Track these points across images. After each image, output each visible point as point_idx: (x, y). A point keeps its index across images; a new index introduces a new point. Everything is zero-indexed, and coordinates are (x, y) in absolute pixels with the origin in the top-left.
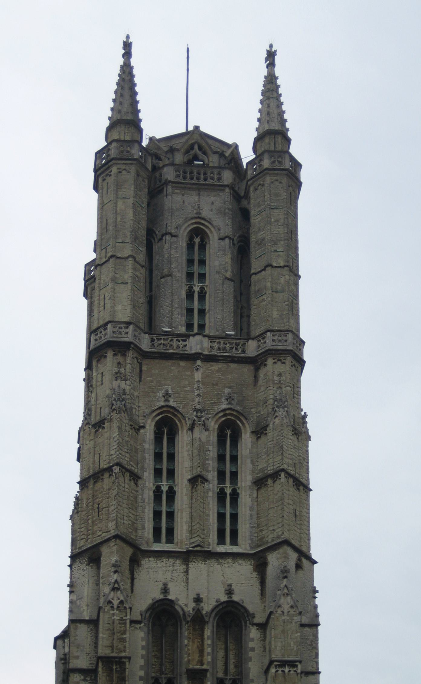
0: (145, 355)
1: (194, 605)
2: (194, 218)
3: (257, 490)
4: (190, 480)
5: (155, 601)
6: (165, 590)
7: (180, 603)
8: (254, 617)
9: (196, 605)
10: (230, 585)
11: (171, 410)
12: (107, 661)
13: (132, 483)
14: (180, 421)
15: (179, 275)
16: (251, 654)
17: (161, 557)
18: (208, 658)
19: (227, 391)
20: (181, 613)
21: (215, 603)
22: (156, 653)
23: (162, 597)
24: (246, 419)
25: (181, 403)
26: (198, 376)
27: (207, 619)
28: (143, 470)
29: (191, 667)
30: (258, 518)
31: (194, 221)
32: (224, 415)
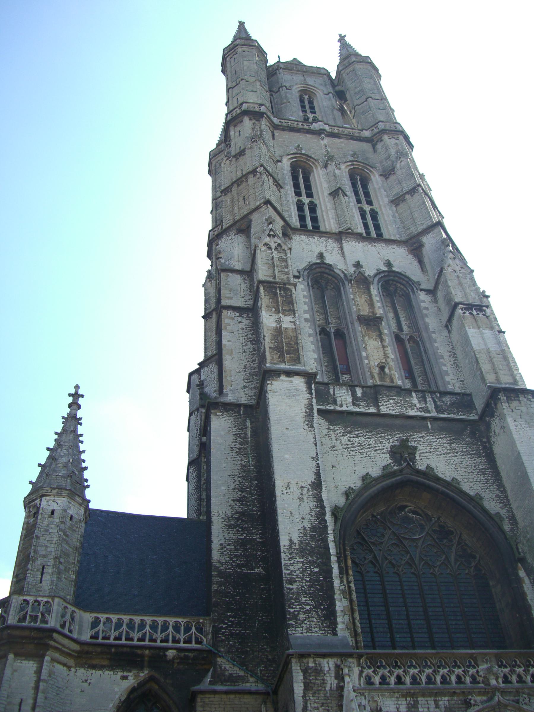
2: (302, 84)
3: (396, 206)
5: (311, 263)
8: (420, 285)
14: (313, 163)
16: (425, 312)
17: (313, 236)
20: (342, 275)
21: (376, 272)
22: (318, 309)
24: (372, 168)
30: (402, 222)
31: (302, 86)
32: (352, 165)
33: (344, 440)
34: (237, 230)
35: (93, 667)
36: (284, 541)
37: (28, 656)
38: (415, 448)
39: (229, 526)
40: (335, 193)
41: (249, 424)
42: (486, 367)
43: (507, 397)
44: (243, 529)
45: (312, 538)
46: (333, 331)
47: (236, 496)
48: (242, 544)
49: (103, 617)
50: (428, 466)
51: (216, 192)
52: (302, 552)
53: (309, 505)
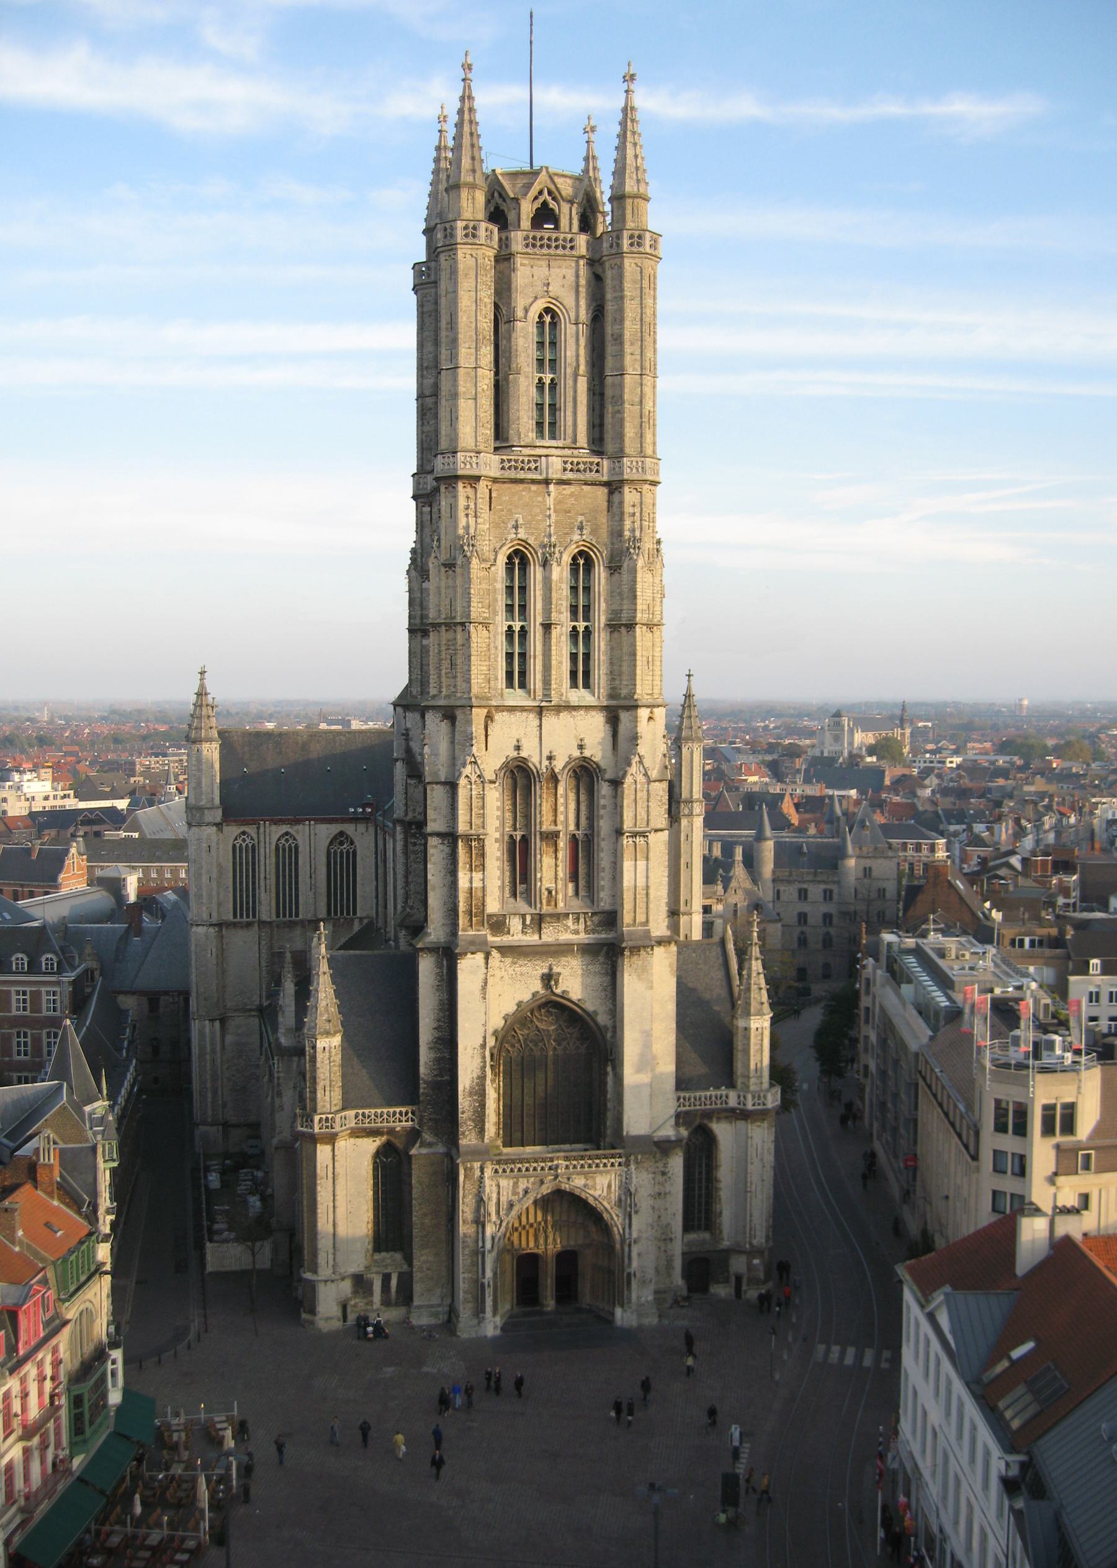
0: (495, 480)
1: (545, 763)
4: (542, 624)
6: (518, 748)
7: (535, 760)
9: (550, 763)
10: (581, 740)
11: (523, 543)
12: (468, 839)
13: (485, 632)
15: (527, 369)
16: (602, 812)
18: (561, 818)
19: (580, 518)
20: (535, 771)
23: (515, 754)
25: (532, 534)
26: (550, 501)
27: (559, 777)
28: (495, 613)
29: (544, 828)
32: (578, 547)
33: (511, 971)
34: (443, 715)
35: (358, 1137)
36: (460, 1088)
37: (326, 1143)
38: (559, 974)
39: (430, 1048)
40: (547, 627)
41: (445, 962)
42: (628, 906)
43: (631, 952)
44: (439, 1049)
45: (477, 1084)
46: (518, 838)
47: (435, 1025)
48: (438, 1060)
49: (361, 1112)
50: (564, 992)
51: (422, 370)
52: (471, 1094)
53: (478, 1061)
